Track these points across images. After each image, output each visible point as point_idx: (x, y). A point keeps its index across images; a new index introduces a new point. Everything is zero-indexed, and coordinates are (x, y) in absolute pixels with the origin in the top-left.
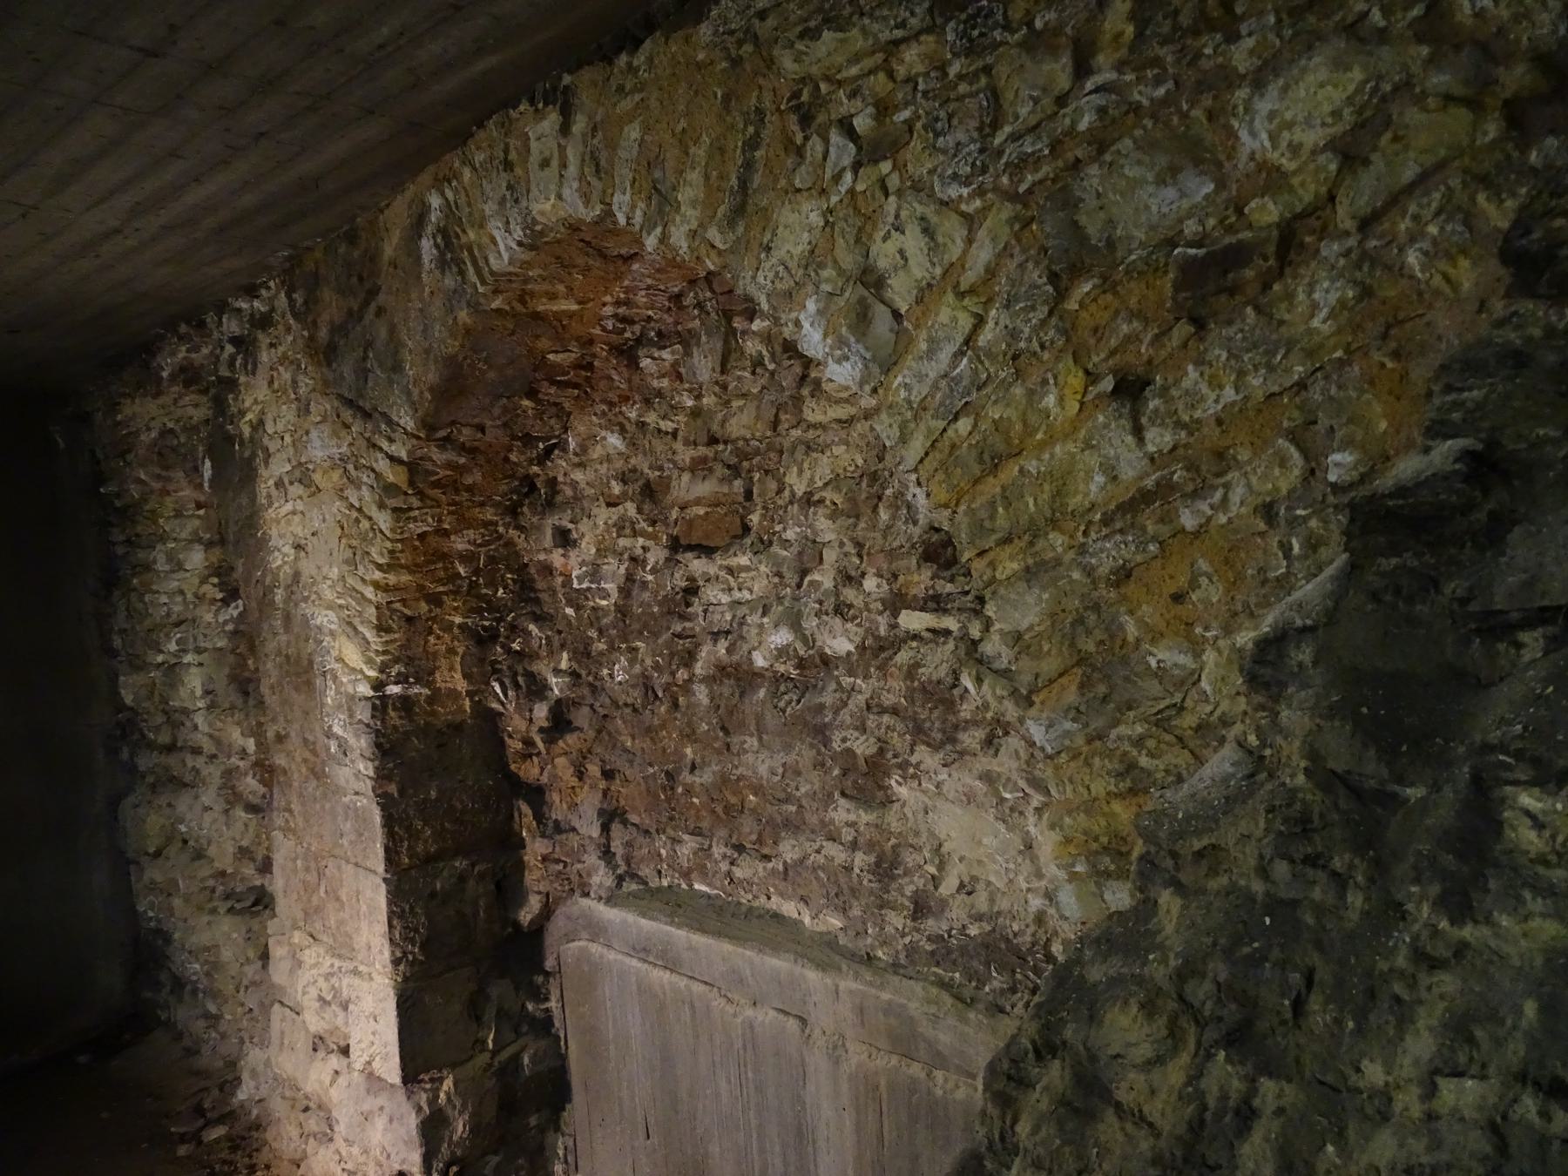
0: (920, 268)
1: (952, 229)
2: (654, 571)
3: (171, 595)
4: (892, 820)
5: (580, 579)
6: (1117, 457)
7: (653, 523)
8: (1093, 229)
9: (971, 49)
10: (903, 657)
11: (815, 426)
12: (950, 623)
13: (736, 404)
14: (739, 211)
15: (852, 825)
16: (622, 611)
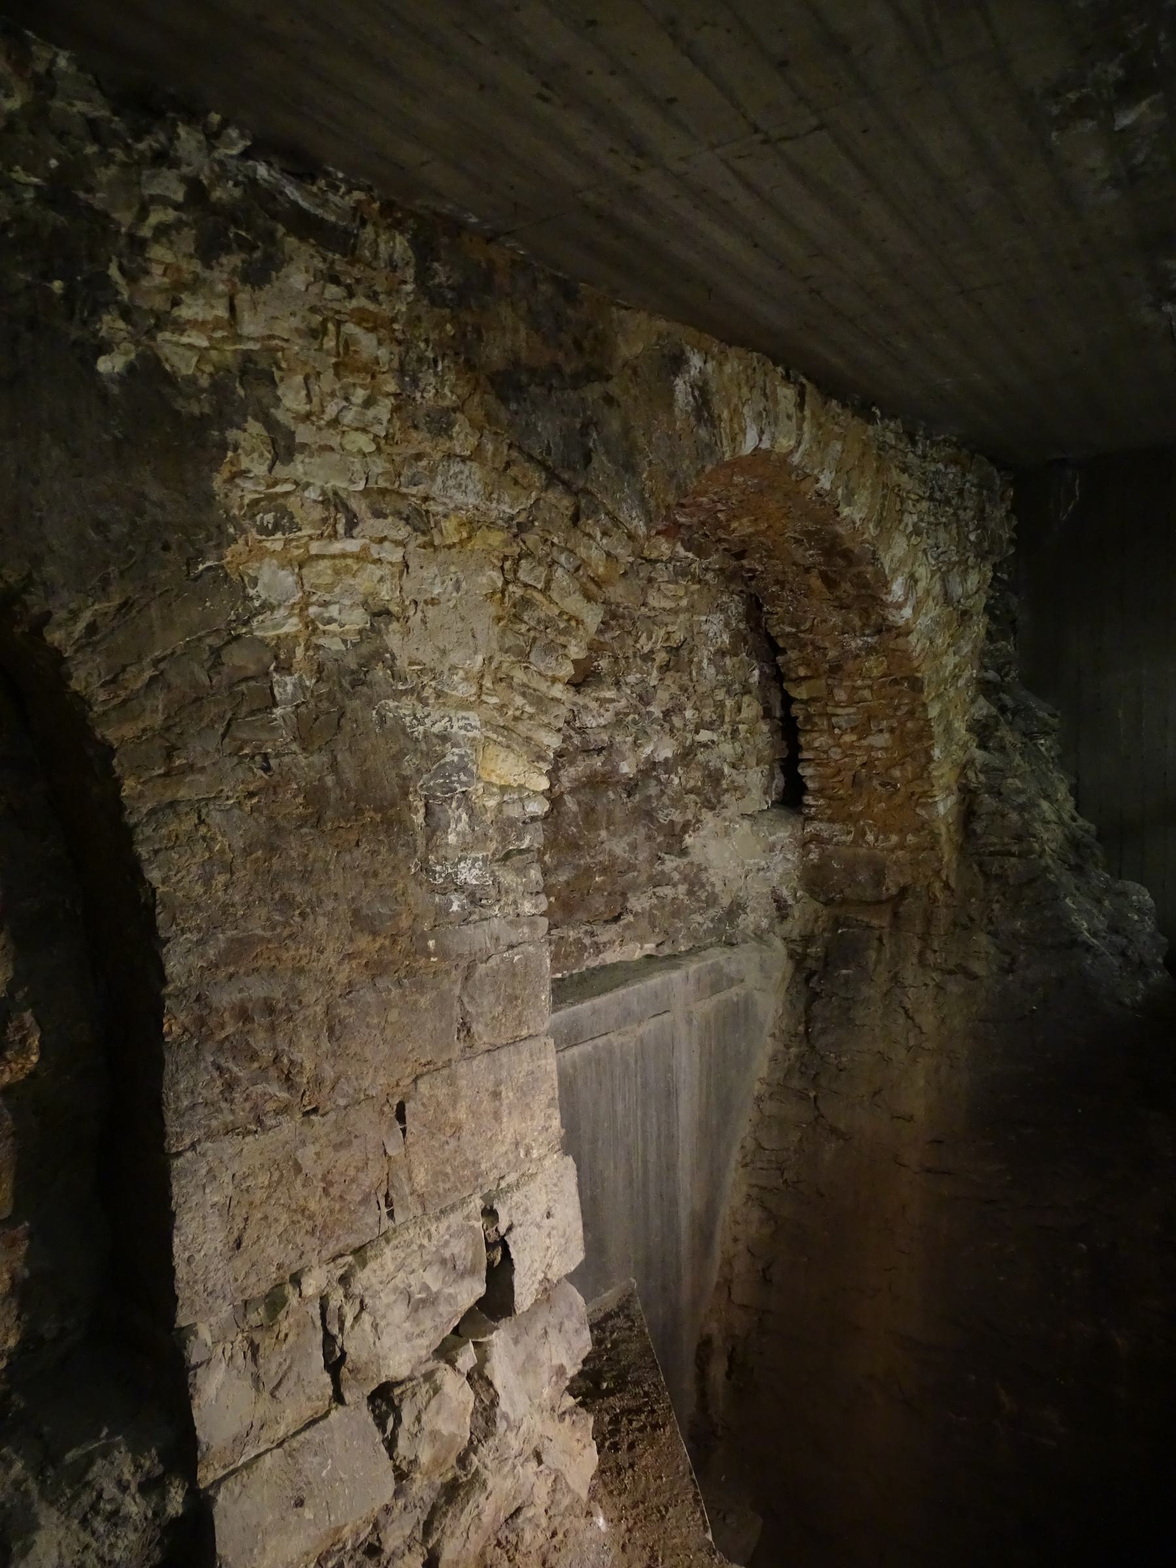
10: (700, 757)
15: (675, 869)
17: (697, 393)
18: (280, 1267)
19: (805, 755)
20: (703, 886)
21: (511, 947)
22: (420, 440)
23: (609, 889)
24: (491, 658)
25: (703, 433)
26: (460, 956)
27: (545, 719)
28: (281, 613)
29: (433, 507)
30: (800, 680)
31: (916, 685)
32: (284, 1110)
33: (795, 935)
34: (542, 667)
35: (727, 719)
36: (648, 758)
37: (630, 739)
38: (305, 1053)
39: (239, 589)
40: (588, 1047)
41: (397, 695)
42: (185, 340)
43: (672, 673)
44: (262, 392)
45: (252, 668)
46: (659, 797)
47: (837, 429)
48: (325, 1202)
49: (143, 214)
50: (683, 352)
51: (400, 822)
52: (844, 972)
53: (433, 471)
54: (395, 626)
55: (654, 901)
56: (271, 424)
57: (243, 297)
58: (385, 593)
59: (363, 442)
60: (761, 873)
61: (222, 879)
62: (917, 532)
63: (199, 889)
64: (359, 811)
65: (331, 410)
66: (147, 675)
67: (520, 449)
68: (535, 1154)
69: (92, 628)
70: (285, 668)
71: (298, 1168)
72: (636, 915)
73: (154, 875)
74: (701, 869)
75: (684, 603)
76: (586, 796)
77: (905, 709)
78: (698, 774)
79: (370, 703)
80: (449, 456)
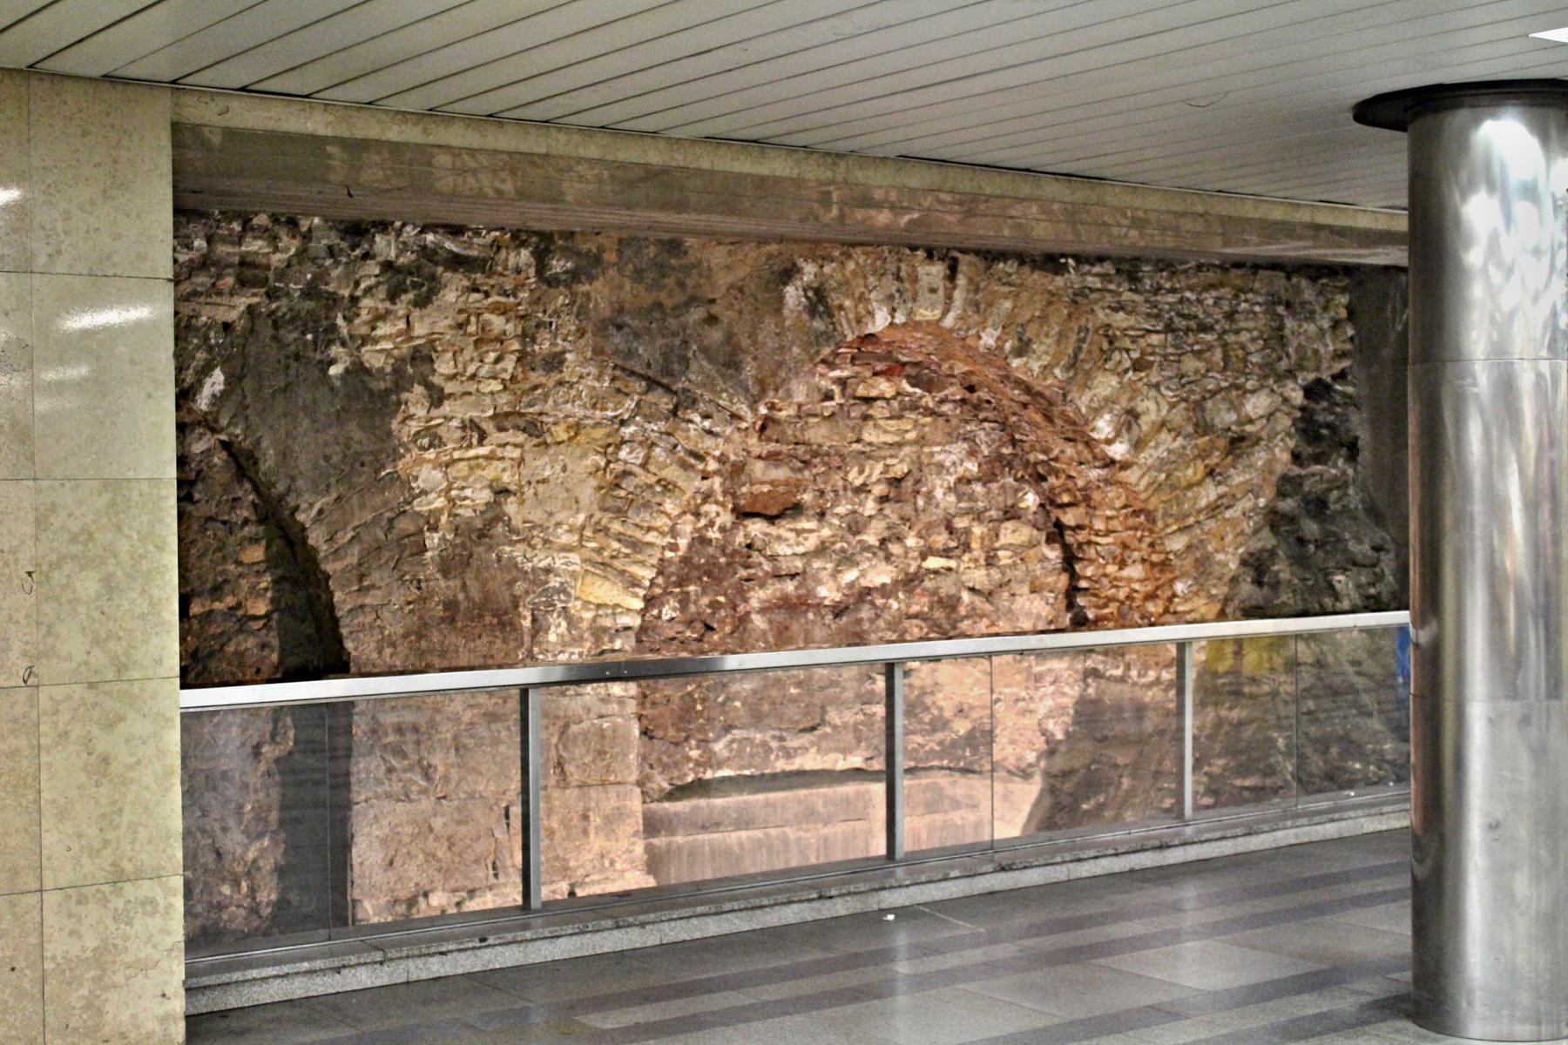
7: (725, 493)
8: (1208, 418)
9: (1176, 347)
10: (928, 584)
11: (870, 444)
12: (952, 564)
13: (813, 420)
14: (1073, 365)
16: (685, 560)
17: (810, 294)
18: (417, 884)
19: (1083, 584)
20: (927, 709)
21: (601, 717)
22: (536, 377)
23: (807, 700)
24: (592, 516)
25: (818, 324)
26: (557, 717)
27: (640, 557)
28: (432, 496)
29: (545, 419)
30: (1063, 506)
31: (1150, 517)
32: (424, 792)
33: (1055, 770)
34: (637, 520)
35: (974, 545)
36: (851, 585)
37: (830, 566)
38: (438, 760)
39: (406, 484)
40: (758, 834)
41: (512, 543)
42: (378, 347)
43: (886, 505)
44: (424, 368)
45: (412, 529)
46: (872, 621)
47: (1007, 289)
48: (449, 855)
49: (357, 284)
50: (794, 265)
51: (511, 624)
52: (1085, 806)
53: (546, 396)
54: (512, 499)
55: (861, 717)
56: (429, 386)
57: (416, 313)
58: (506, 478)
59: (496, 386)
60: (1021, 704)
61: (388, 651)
62: (1137, 366)
63: (375, 655)
64: (481, 616)
65: (471, 369)
66: (349, 536)
67: (623, 369)
68: (618, 866)
69: (321, 512)
70: (434, 528)
71: (431, 829)
72: (835, 727)
73: (349, 645)
74: (923, 693)
75: (911, 436)
76: (781, 616)
77: (1148, 540)
78: (925, 600)
79: (491, 548)
80: (561, 383)
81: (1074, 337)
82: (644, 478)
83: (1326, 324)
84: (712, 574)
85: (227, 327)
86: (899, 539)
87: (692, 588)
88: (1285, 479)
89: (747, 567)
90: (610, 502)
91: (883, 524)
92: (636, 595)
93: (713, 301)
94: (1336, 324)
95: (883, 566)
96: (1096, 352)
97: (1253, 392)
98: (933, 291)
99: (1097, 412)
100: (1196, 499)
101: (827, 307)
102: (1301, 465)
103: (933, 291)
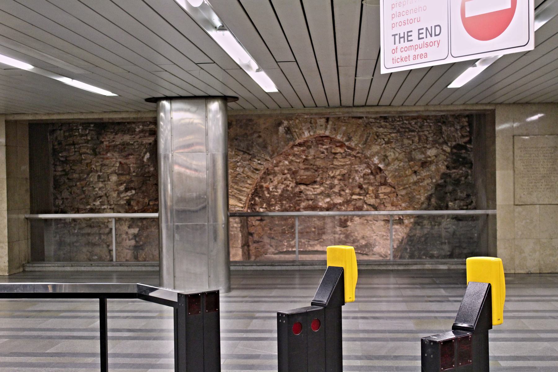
0: (393, 156)
1: (397, 155)
2: (292, 187)
3: (100, 189)
4: (349, 228)
5: (273, 189)
6: (414, 178)
7: (292, 178)
9: (401, 137)
10: (353, 203)
12: (362, 197)
13: (318, 159)
14: (365, 143)
16: (281, 195)
20: (352, 236)
25: (288, 136)
35: (370, 192)
36: (328, 202)
47: (344, 124)
60: (385, 237)
72: (324, 240)
75: (349, 163)
81: (365, 136)
82: (243, 175)
83: (458, 127)
84: (289, 199)
85: (150, 144)
86: (343, 190)
87: (284, 202)
88: (444, 174)
89: (299, 197)
90: (234, 181)
91: (339, 186)
92: (241, 203)
93: (260, 132)
94: (463, 127)
95: (339, 197)
96: (373, 139)
97: (429, 149)
98: (321, 126)
99: (373, 156)
100: (408, 180)
101: (290, 131)
102: (450, 170)
103: (321, 126)
